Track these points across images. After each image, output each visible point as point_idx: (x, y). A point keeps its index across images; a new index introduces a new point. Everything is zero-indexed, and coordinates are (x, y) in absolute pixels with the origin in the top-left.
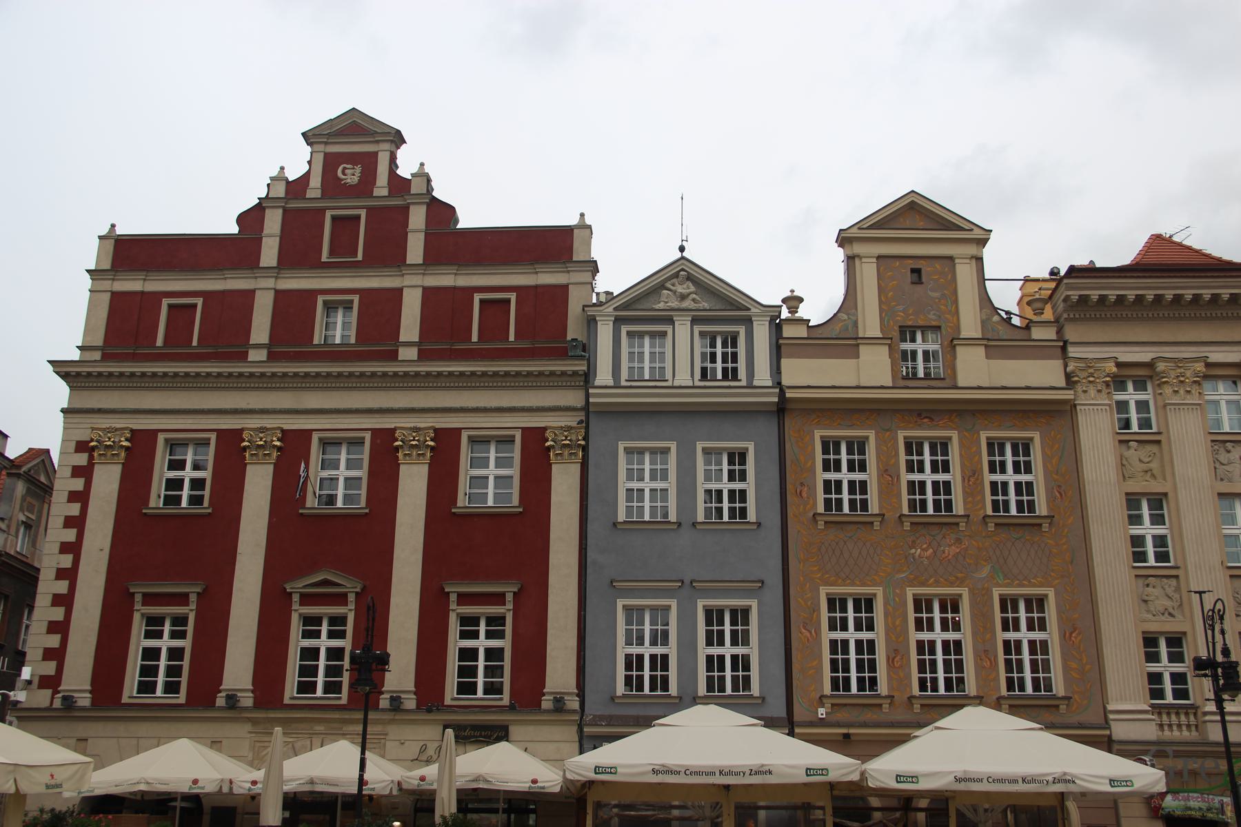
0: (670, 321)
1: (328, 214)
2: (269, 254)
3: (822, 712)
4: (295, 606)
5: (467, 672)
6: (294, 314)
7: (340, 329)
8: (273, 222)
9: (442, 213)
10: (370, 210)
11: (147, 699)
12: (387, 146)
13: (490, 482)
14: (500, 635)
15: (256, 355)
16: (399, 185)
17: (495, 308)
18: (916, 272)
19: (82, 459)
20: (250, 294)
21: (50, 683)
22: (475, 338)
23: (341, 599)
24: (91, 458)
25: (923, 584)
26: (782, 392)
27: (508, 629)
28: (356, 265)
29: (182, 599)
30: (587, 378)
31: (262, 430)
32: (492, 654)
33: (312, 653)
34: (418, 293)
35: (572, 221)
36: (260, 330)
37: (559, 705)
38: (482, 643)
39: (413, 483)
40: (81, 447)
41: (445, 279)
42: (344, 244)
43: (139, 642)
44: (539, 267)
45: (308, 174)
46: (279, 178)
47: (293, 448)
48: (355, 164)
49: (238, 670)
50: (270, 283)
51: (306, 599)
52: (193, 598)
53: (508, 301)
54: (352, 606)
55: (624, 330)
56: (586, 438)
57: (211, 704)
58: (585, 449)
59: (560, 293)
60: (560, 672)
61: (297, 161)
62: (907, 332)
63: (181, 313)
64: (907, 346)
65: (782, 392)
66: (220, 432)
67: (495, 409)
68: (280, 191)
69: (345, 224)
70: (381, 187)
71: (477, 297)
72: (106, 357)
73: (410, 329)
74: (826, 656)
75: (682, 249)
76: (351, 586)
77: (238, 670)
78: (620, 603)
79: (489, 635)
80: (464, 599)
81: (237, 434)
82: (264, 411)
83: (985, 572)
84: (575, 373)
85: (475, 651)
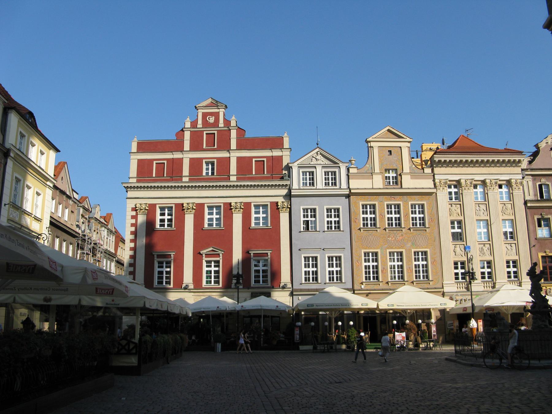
0: (315, 167)
1: (205, 133)
2: (187, 146)
3: (363, 286)
4: (204, 258)
5: (257, 277)
6: (196, 164)
11: (160, 286)
15: (185, 179)
17: (260, 163)
18: (390, 152)
20: (182, 159)
22: (254, 173)
25: (392, 248)
26: (350, 190)
32: (264, 271)
36: (186, 171)
39: (237, 219)
47: (199, 210)
48: (212, 116)
51: (207, 255)
53: (264, 161)
54: (221, 257)
55: (301, 170)
58: (290, 209)
59: (280, 158)
62: (388, 170)
63: (160, 166)
64: (387, 175)
65: (350, 190)
66: (176, 204)
68: (188, 125)
70: (221, 124)
71: (254, 160)
72: (138, 181)
74: (364, 270)
75: (317, 144)
82: (189, 197)
83: (409, 244)
84: (286, 185)
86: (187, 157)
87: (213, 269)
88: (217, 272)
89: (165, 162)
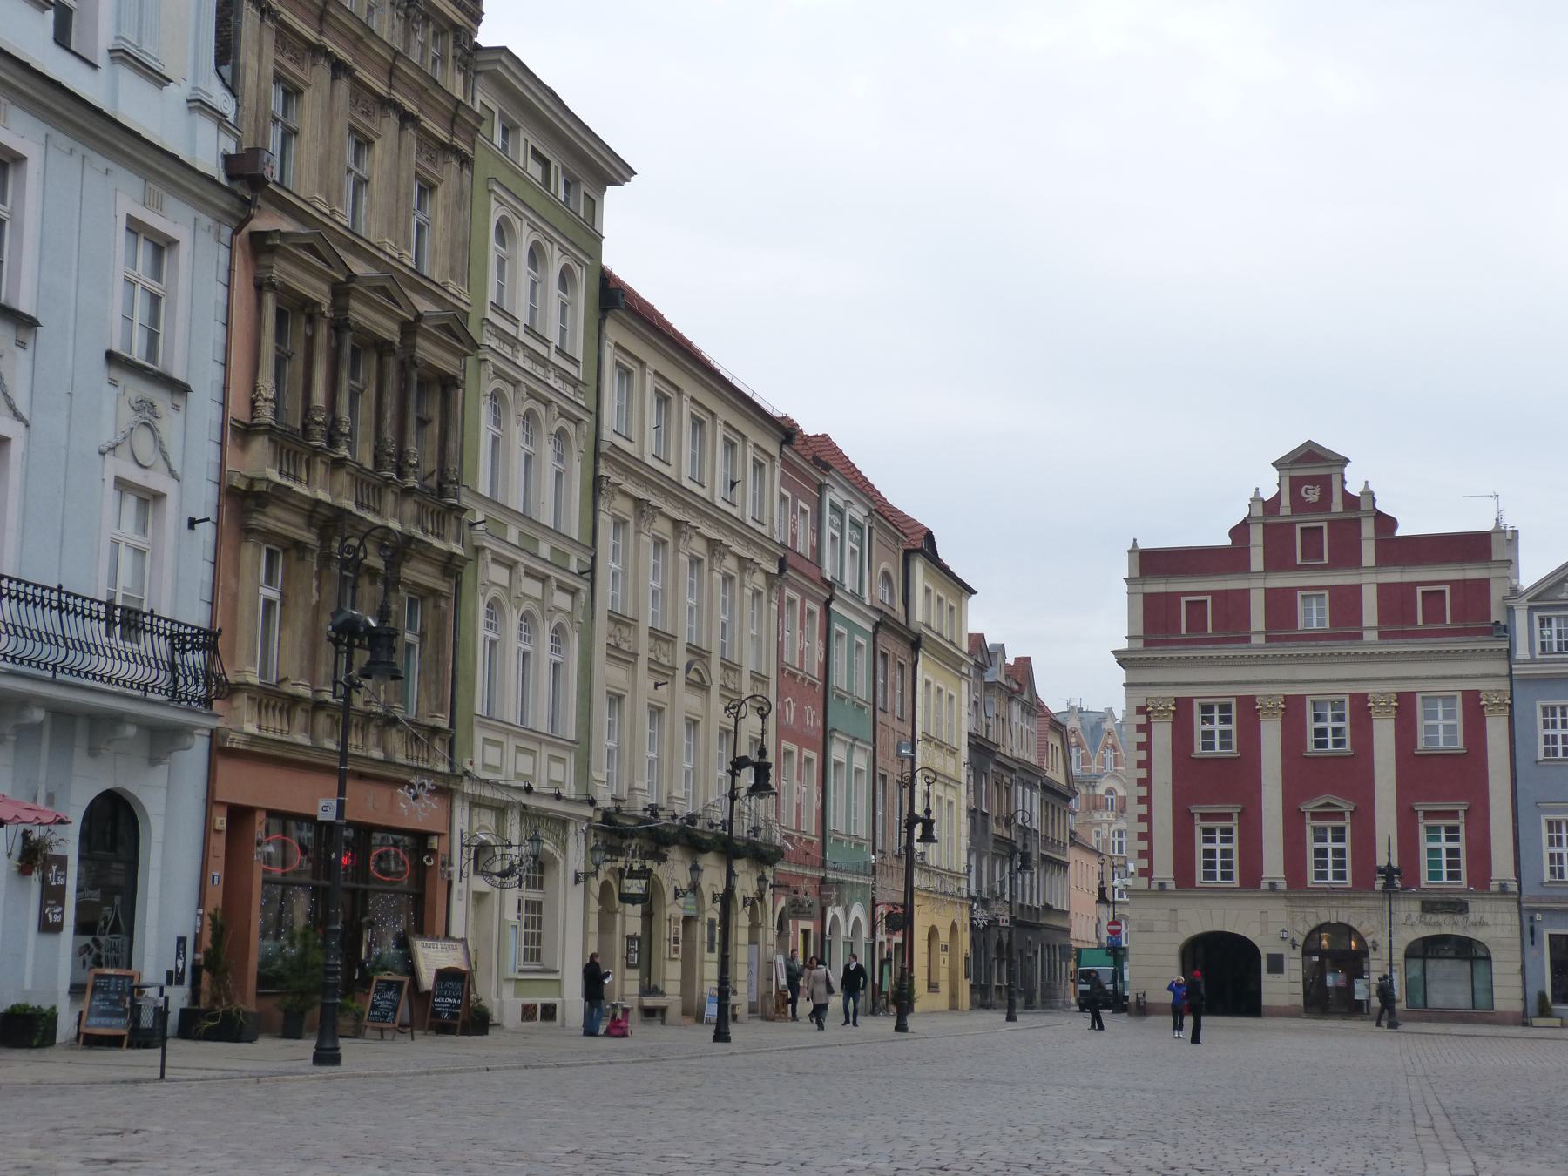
1: (1298, 527)
2: (1257, 560)
7: (1314, 616)
8: (1257, 535)
9: (1386, 523)
10: (1331, 523)
11: (1210, 883)
12: (1337, 470)
13: (1441, 731)
14: (1456, 839)
15: (1257, 640)
16: (1351, 501)
19: (1142, 719)
20: (1245, 593)
21: (1147, 873)
23: (1341, 815)
24: (1149, 719)
27: (1462, 834)
28: (1323, 567)
29: (1228, 817)
30: (1509, 654)
31: (1270, 696)
33: (1321, 853)
34: (1374, 589)
35: (1488, 526)
36: (1258, 620)
37: (1503, 889)
38: (1444, 845)
39: (1384, 733)
40: (1141, 710)
41: (1394, 576)
42: (1312, 550)
43: (1200, 846)
44: (1467, 566)
45: (1278, 494)
46: (1256, 499)
47: (1293, 709)
49: (1273, 864)
50: (1260, 583)
51: (1315, 816)
52: (1235, 816)
55: (1536, 615)
56: (1511, 698)
57: (1257, 886)
58: (1511, 706)
59: (1483, 586)
60: (1502, 867)
61: (1270, 485)
66: (1239, 699)
67: (1439, 678)
68: (1259, 511)
69: (1312, 534)
70: (1337, 506)
72: (1147, 643)
73: (1370, 615)
76: (1346, 806)
77: (1273, 864)
78: (1544, 819)
79: (1448, 839)
80: (1428, 815)
81: (1251, 700)
82: (1269, 681)
85: (1439, 850)
86: (1257, 585)
87: (1330, 845)
88: (1339, 853)
89: (1209, 598)
